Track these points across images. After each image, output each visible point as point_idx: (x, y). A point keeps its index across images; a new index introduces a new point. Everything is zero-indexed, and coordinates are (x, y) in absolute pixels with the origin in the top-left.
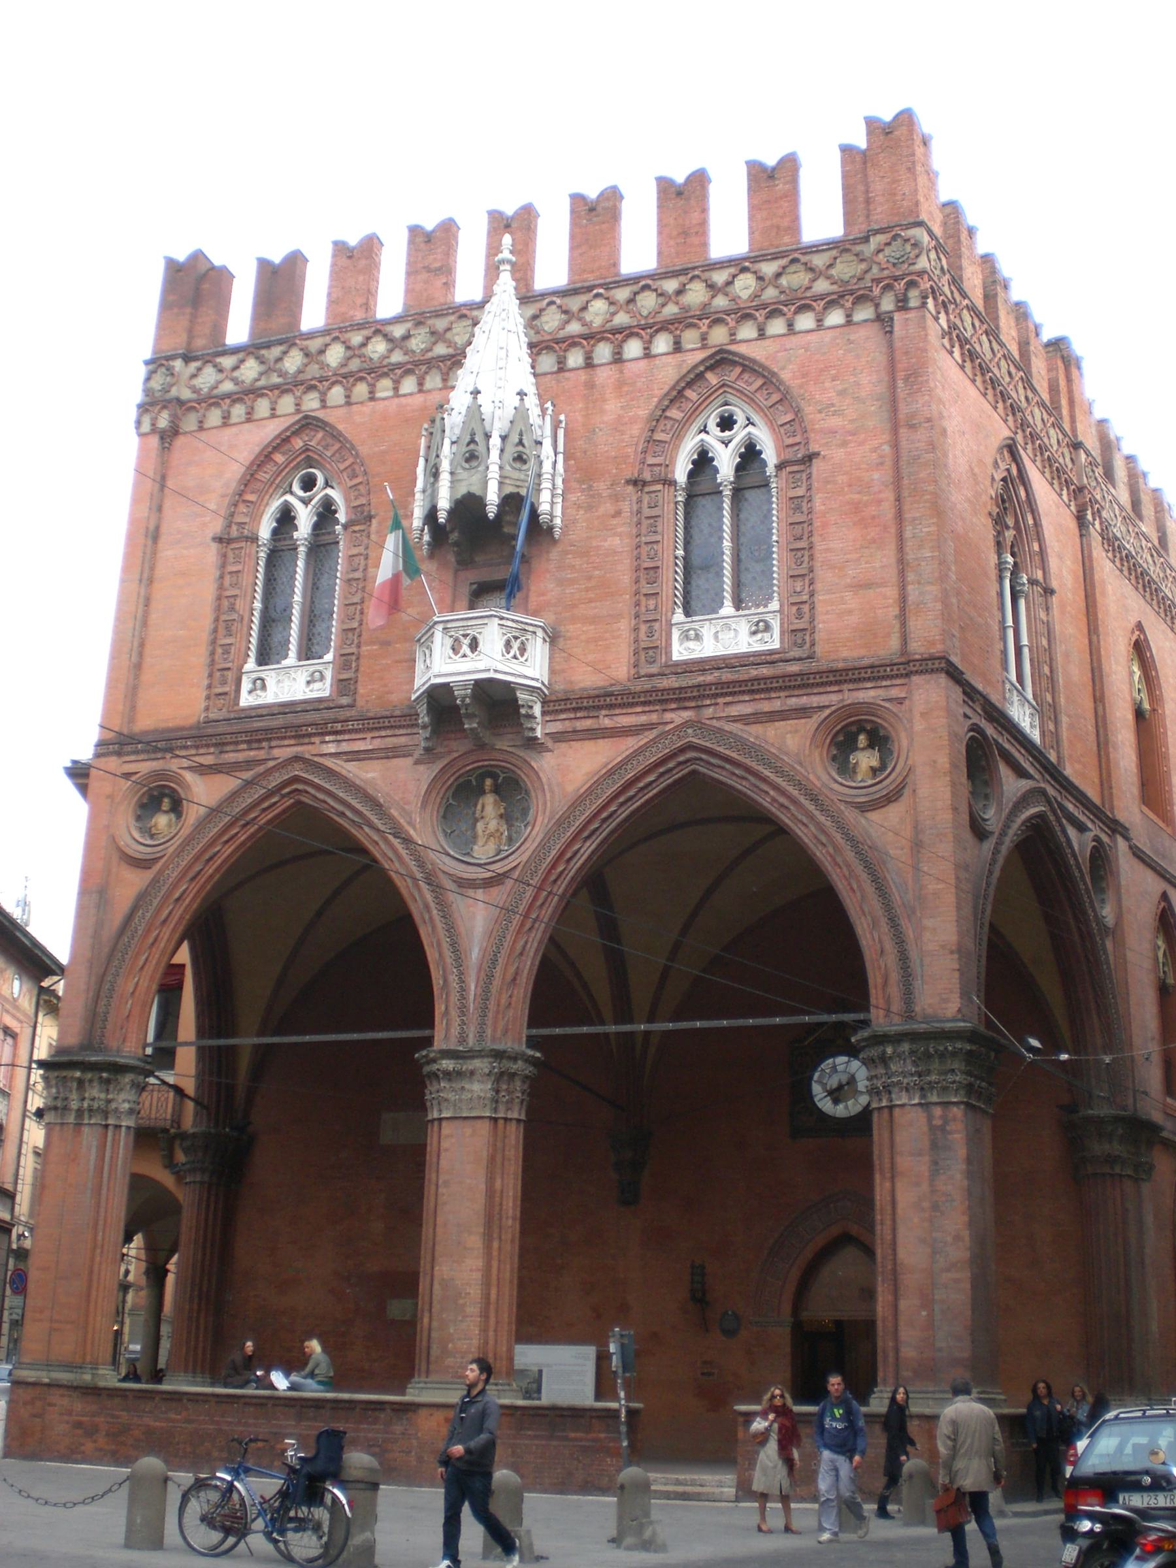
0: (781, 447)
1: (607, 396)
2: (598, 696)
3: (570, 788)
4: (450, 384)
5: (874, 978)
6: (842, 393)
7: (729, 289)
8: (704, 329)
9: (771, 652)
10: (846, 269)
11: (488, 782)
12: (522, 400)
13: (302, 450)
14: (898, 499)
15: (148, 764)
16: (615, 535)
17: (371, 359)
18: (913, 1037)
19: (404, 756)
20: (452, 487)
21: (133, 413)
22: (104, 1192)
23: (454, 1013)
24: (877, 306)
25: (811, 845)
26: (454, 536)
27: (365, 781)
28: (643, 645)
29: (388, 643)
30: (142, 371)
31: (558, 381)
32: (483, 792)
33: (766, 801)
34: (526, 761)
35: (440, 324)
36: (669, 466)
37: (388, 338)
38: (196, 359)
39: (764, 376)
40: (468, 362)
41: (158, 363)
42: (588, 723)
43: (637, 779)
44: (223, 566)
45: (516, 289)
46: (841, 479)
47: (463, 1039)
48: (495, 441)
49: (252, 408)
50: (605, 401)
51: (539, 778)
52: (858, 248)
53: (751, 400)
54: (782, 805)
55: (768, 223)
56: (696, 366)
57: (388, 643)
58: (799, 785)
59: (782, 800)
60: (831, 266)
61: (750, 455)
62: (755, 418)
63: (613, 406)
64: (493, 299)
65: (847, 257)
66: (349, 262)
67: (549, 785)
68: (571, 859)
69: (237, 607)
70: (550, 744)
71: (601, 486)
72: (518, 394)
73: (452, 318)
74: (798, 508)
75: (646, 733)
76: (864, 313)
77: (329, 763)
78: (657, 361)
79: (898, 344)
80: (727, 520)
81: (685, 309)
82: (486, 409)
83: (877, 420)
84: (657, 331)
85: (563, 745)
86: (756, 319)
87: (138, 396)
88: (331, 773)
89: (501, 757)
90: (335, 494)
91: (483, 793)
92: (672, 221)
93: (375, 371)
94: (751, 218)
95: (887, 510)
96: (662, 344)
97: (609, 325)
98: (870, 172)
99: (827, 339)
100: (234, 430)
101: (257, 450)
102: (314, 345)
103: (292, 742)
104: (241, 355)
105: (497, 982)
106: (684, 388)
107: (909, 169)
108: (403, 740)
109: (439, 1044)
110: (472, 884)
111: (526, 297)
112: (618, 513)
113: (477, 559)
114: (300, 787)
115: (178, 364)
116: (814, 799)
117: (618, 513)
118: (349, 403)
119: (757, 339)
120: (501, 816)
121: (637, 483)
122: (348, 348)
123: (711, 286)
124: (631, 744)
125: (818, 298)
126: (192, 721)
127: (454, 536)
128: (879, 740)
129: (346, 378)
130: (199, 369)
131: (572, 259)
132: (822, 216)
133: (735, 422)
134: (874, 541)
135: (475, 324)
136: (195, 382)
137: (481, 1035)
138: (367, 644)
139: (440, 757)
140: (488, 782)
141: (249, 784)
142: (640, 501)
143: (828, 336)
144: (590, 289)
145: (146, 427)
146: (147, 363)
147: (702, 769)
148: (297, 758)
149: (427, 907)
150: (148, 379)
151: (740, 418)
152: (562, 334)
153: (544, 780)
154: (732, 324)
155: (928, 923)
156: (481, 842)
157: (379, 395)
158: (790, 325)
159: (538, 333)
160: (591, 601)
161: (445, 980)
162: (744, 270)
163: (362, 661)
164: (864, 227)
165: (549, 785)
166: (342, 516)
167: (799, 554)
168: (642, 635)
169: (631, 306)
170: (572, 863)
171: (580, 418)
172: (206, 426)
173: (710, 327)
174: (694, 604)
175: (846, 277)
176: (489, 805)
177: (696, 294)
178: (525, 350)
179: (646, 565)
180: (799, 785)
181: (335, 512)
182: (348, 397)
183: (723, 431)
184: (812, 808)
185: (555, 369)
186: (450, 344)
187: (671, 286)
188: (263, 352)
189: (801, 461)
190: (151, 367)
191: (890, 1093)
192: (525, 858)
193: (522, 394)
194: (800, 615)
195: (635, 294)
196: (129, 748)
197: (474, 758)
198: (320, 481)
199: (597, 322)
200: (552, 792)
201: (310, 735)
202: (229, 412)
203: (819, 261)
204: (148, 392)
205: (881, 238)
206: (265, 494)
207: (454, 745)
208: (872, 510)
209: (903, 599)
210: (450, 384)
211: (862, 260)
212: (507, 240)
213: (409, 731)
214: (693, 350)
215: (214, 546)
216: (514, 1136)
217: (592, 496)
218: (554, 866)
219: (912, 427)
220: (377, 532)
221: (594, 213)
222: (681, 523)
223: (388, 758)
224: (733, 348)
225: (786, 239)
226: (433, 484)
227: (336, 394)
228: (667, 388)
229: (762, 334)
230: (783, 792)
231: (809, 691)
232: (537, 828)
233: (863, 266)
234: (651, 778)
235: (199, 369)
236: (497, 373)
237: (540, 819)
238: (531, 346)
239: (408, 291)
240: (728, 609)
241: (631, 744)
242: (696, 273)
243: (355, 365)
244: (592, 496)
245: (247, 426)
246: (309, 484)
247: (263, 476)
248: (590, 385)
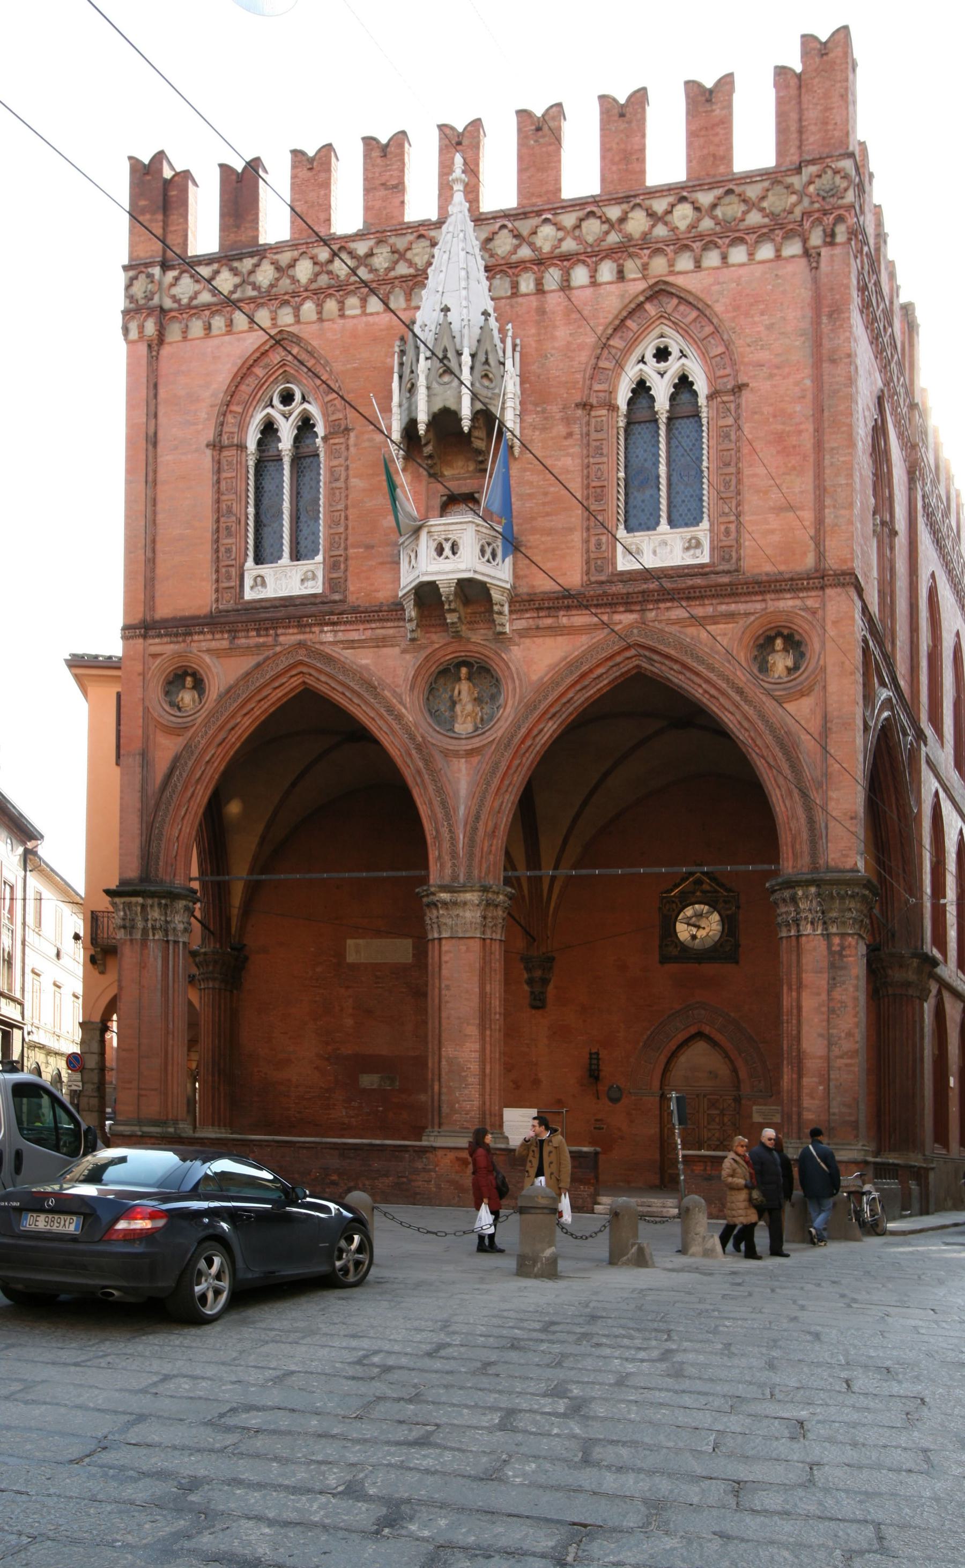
0: (712, 379)
1: (557, 323)
2: (557, 598)
3: (534, 678)
4: (413, 304)
5: (785, 838)
6: (770, 327)
7: (668, 218)
8: (645, 259)
9: (702, 566)
10: (777, 201)
11: (464, 670)
12: (486, 320)
13: (282, 362)
14: (818, 430)
15: (172, 646)
16: (568, 455)
17: (338, 276)
18: (818, 883)
19: (392, 646)
20: (429, 402)
21: (118, 320)
22: (171, 992)
23: (447, 858)
24: (805, 241)
25: (735, 730)
26: (428, 450)
27: (361, 666)
28: (592, 556)
29: (373, 547)
30: (121, 279)
31: (512, 306)
33: (698, 692)
35: (401, 243)
36: (612, 392)
37: (351, 253)
38: (172, 268)
39: (698, 309)
40: (430, 283)
41: (135, 268)
42: (549, 621)
43: (591, 671)
44: (219, 471)
45: (469, 210)
46: (767, 410)
47: (455, 878)
48: (466, 359)
49: (231, 321)
50: (555, 327)
51: (509, 668)
52: (789, 180)
53: (684, 331)
54: (712, 696)
55: (705, 151)
56: (637, 296)
57: (373, 547)
58: (728, 681)
59: (713, 692)
60: (763, 198)
61: (684, 383)
62: (687, 351)
63: (562, 333)
64: (449, 220)
65: (779, 189)
66: (310, 174)
67: (518, 674)
69: (234, 509)
70: (517, 639)
71: (554, 409)
72: (483, 314)
73: (411, 238)
74: (727, 436)
75: (599, 632)
76: (793, 248)
77: (327, 650)
78: (602, 290)
79: (824, 280)
80: (663, 446)
81: (629, 238)
82: (455, 327)
83: (800, 352)
84: (602, 259)
85: (527, 641)
86: (693, 250)
87: (120, 303)
88: (329, 659)
89: (476, 649)
90: (314, 410)
91: (460, 679)
92: (615, 146)
93: (341, 289)
94: (690, 145)
95: (807, 441)
96: (607, 271)
97: (557, 251)
98: (805, 98)
99: (758, 274)
100: (216, 341)
101: (240, 362)
102: (285, 258)
103: (295, 631)
104: (215, 266)
105: (481, 833)
106: (626, 318)
107: (842, 96)
108: (391, 632)
109: (434, 878)
110: (456, 754)
111: (479, 220)
112: (570, 435)
113: (446, 473)
114: (305, 670)
115: (156, 271)
116: (740, 692)
117: (570, 435)
118: (321, 320)
119: (693, 272)
120: (475, 699)
121: (586, 406)
122: (315, 263)
123: (651, 214)
124: (583, 642)
125: (751, 230)
126: (205, 611)
127: (428, 450)
128: (794, 643)
129: (319, 295)
130: (177, 279)
131: (521, 182)
132: (754, 145)
133: (670, 354)
134: (794, 468)
135: (434, 244)
136: (174, 291)
137: (469, 875)
138: (354, 546)
139: (422, 647)
141: (258, 665)
142: (588, 424)
143: (758, 270)
144: (539, 213)
145: (134, 334)
146: (126, 268)
147: (644, 665)
148: (301, 644)
149: (419, 772)
150: (129, 286)
151: (674, 350)
152: (514, 258)
153: (513, 669)
154: (671, 255)
155: (833, 794)
156: (460, 720)
157: (348, 313)
158: (724, 257)
159: (492, 256)
160: (548, 514)
161: (437, 831)
162: (683, 199)
163: (349, 562)
164: (796, 159)
165: (518, 674)
166: (320, 430)
167: (727, 478)
168: (592, 548)
169: (577, 233)
170: (538, 739)
171: (534, 344)
172: (189, 337)
173: (650, 257)
174: (632, 521)
175: (777, 210)
176: (464, 689)
177: (637, 223)
178: (482, 275)
179: (594, 484)
180: (728, 681)
181: (314, 426)
182: (320, 313)
183: (658, 362)
184: (738, 698)
185: (509, 294)
186: (411, 264)
187: (614, 212)
188: (235, 264)
189: (730, 391)
190: (131, 273)
191: (798, 925)
192: (500, 734)
193: (486, 314)
194: (727, 533)
195: (581, 220)
196: (151, 633)
197: (450, 649)
198: (298, 397)
199: (546, 249)
200: (520, 680)
201: (310, 625)
202: (210, 324)
203: (752, 192)
204: (130, 298)
205: (813, 169)
206: (258, 397)
207: (434, 637)
208: (793, 440)
209: (820, 522)
210: (413, 304)
211: (793, 193)
212: (458, 159)
213: (396, 624)
214: (634, 280)
215: (209, 452)
216: (497, 951)
217: (546, 419)
218: (523, 742)
219: (833, 361)
220: (356, 445)
221: (540, 133)
222: (622, 448)
223: (378, 647)
224: (670, 279)
225: (722, 169)
226: (409, 399)
227: (309, 308)
228: (611, 317)
229: (698, 266)
230: (714, 686)
231: (737, 599)
232: (508, 710)
233: (794, 198)
234: (601, 670)
235: (177, 279)
236: (457, 292)
237: (510, 703)
238: (487, 269)
239: (367, 209)
240: (664, 526)
241: (583, 642)
242: (638, 201)
243: (324, 280)
244: (546, 419)
245: (227, 338)
246: (287, 398)
247: (245, 389)
248: (541, 311)
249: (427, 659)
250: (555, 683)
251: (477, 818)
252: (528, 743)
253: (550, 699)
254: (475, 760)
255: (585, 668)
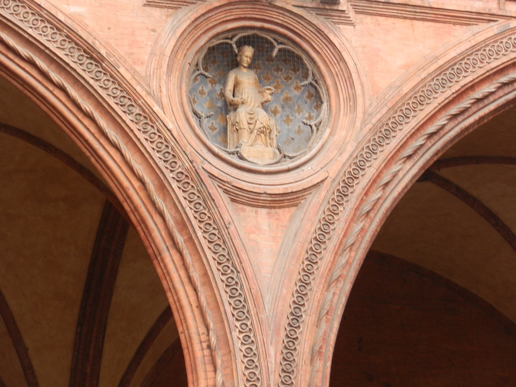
32: (236, 64)
34: (319, 31)
68: (387, 184)
75: (483, 26)
85: (368, 19)
89: (279, 18)
140: (248, 52)
232: (340, 134)
249: (195, 23)
250: (417, 97)
251: (295, 318)
252: (374, 196)
253: (413, 123)
254: (285, 214)
255: (465, 80)
